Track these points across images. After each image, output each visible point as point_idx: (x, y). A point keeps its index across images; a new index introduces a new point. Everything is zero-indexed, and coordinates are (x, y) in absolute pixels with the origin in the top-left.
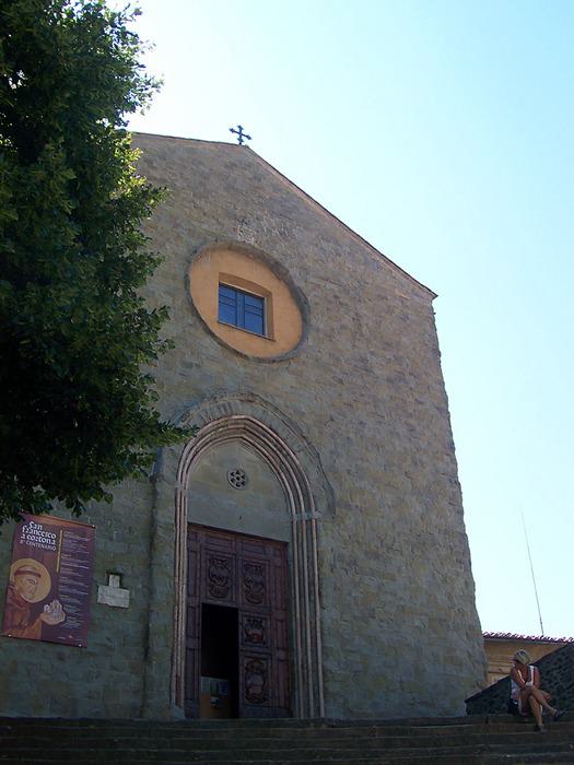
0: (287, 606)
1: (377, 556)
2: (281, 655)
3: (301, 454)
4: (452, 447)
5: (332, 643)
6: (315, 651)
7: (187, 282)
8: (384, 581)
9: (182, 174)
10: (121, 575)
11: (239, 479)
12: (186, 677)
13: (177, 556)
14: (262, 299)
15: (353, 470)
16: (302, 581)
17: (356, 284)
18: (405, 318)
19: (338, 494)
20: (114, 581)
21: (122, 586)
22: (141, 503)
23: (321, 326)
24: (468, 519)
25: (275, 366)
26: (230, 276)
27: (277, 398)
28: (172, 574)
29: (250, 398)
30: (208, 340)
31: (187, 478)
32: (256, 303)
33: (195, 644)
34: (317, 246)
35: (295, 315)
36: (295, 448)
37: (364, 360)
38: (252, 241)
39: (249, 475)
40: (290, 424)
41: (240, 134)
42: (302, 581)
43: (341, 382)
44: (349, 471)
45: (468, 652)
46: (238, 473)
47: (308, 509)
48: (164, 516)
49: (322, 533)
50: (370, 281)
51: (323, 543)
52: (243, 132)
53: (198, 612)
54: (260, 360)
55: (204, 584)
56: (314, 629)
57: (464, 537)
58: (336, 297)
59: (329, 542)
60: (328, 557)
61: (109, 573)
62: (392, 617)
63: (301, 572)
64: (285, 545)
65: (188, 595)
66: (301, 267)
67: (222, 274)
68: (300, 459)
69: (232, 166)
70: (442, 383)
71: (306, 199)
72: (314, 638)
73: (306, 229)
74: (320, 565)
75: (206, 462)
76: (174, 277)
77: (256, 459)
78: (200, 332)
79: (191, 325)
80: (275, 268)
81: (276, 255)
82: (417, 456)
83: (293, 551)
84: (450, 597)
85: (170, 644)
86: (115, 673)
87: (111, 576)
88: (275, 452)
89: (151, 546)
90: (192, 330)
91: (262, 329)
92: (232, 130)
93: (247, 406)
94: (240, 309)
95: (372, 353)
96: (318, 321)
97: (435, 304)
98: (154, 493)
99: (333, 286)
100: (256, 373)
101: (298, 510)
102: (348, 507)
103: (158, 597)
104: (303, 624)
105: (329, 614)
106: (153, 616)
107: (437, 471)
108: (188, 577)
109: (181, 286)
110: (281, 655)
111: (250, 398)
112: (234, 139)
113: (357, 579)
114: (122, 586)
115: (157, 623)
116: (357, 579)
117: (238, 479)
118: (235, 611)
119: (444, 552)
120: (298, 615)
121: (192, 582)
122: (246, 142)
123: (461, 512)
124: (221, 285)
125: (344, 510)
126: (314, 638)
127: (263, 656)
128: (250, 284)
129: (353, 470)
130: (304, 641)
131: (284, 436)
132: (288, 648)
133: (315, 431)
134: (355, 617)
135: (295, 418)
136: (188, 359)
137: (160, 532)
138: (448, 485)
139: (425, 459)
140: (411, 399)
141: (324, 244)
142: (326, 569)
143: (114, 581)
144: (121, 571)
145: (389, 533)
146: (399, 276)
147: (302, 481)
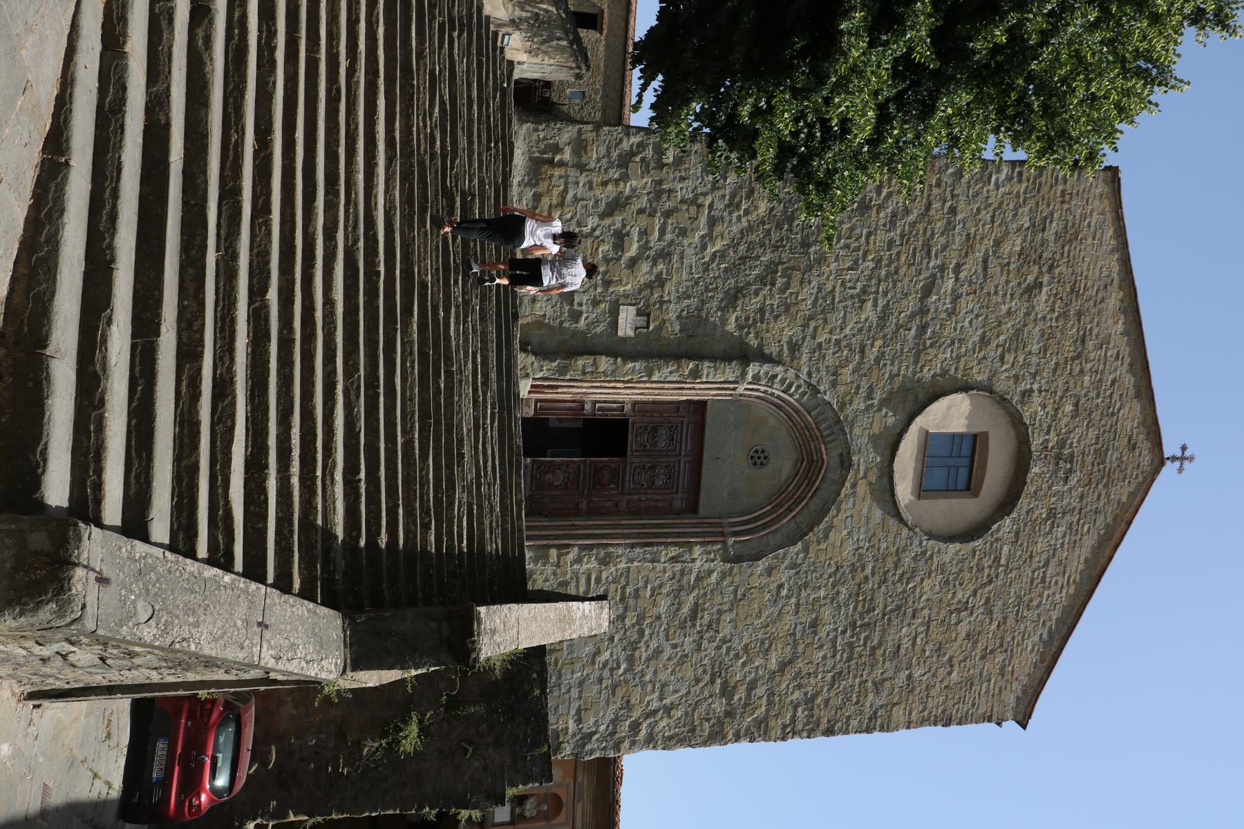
0: (635, 512)
2: (584, 505)
3: (793, 525)
14: (968, 488)
20: (641, 321)
25: (888, 497)
28: (655, 378)
32: (962, 483)
36: (799, 519)
38: (1035, 470)
41: (1183, 459)
45: (595, 733)
46: (765, 458)
47: (735, 534)
52: (1186, 463)
64: (693, 508)
65: (635, 403)
71: (1113, 543)
75: (772, 421)
77: (784, 475)
79: (917, 396)
90: (911, 398)
92: (1184, 448)
94: (951, 462)
108: (654, 402)
110: (584, 505)
112: (1170, 449)
118: (623, 453)
124: (975, 436)
128: (983, 468)
131: (812, 505)
132: (593, 512)
134: (623, 588)
142: (673, 551)
147: (765, 526)
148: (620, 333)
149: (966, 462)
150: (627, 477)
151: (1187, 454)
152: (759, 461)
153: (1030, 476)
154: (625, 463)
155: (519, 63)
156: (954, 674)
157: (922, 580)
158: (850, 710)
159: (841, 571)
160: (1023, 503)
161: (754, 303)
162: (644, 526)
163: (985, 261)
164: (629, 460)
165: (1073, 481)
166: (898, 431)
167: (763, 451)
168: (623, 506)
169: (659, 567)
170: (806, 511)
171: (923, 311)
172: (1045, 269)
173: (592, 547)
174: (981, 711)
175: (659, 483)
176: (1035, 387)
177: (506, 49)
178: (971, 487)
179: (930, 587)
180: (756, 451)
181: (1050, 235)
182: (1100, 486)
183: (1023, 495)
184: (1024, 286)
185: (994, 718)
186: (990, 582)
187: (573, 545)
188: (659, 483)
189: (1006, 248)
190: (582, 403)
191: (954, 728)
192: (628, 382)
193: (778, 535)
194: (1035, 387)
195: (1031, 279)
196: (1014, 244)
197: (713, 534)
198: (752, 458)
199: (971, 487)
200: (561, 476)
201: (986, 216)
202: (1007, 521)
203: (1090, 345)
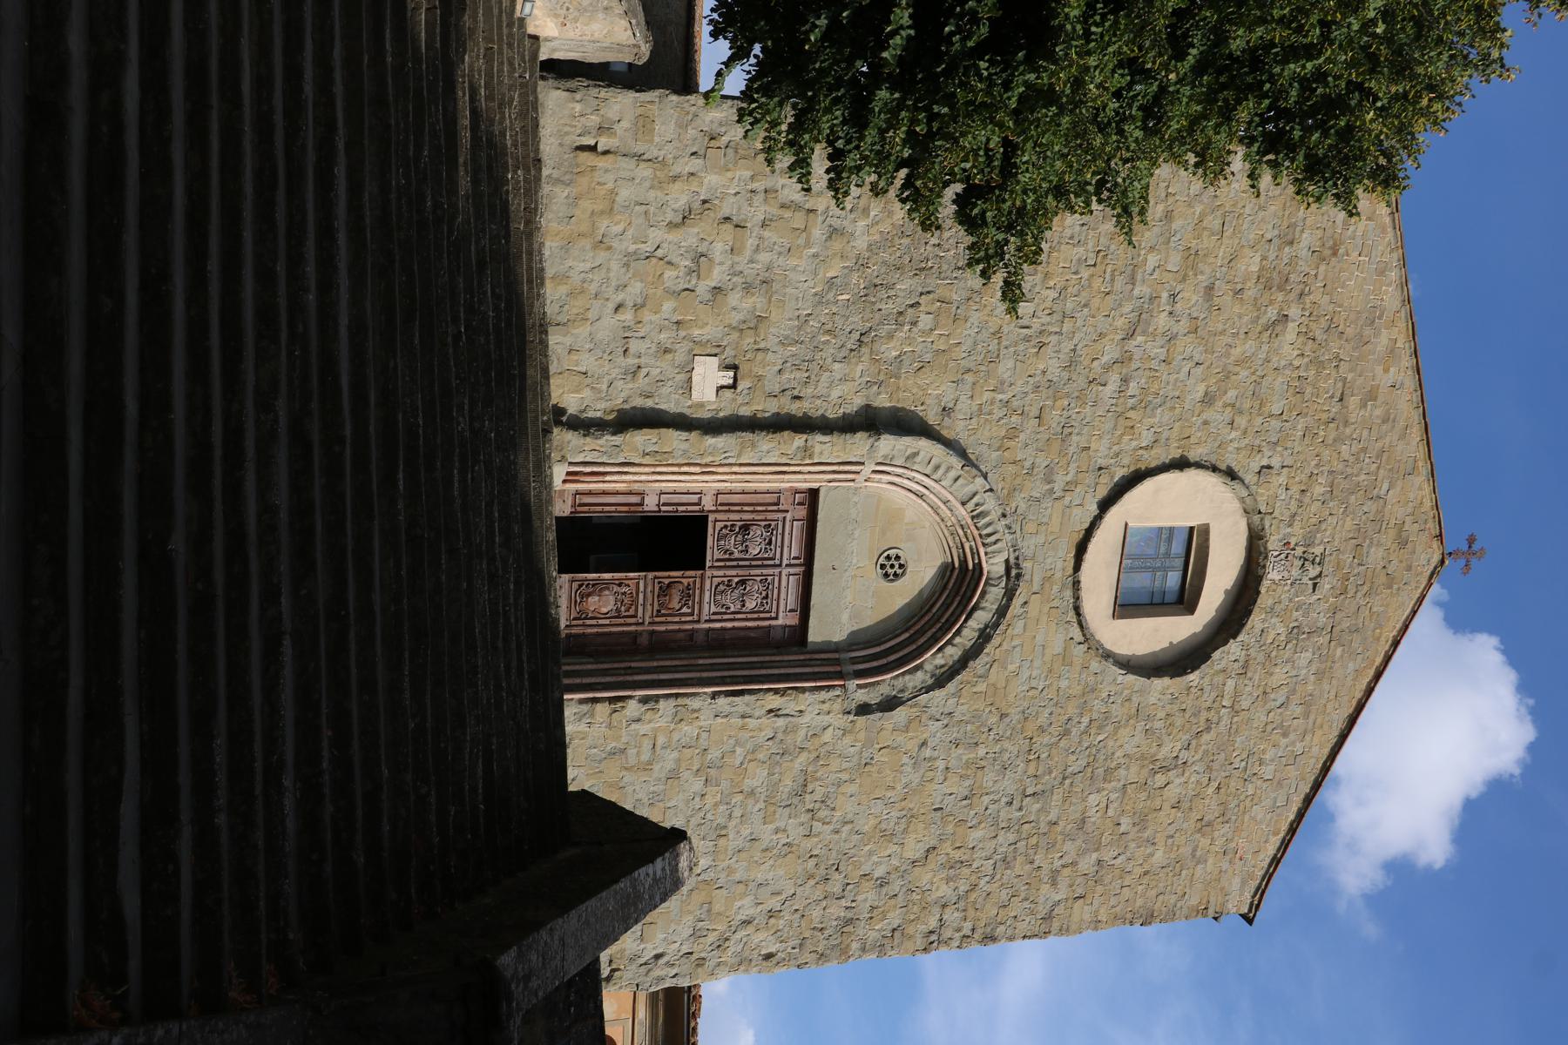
1: (802, 790)
7: (1181, 464)
8: (761, 805)
9: (1364, 450)
10: (734, 386)
15: (928, 753)
16: (751, 666)
20: (727, 378)
25: (1071, 616)
27: (1021, 624)
31: (880, 485)
33: (651, 504)
40: (985, 636)
42: (751, 666)
43: (1066, 733)
44: (924, 744)
46: (901, 566)
48: (826, 447)
49: (823, 695)
51: (808, 697)
62: (709, 816)
63: (762, 665)
66: (1246, 666)
67: (1205, 531)
73: (1320, 675)
74: (776, 691)
78: (1103, 492)
84: (747, 922)
86: (604, 387)
87: (731, 374)
88: (938, 620)
92: (1471, 541)
99: (1225, 721)
104: (687, 669)
107: (944, 906)
111: (1014, 572)
113: (761, 756)
115: (674, 440)
117: (892, 566)
119: (816, 913)
120: (701, 662)
124: (1192, 529)
125: (862, 735)
127: (640, 609)
129: (928, 753)
131: (965, 632)
133: (981, 687)
137: (799, 440)
138: (923, 928)
142: (774, 701)
143: (727, 378)
144: (739, 388)
149: (1179, 563)
150: (707, 598)
151: (1475, 547)
152: (890, 571)
153: (1265, 583)
154: (702, 577)
155: (547, 40)
156: (1159, 854)
157: (1116, 730)
158: (1017, 908)
159: (1007, 720)
160: (1256, 620)
161: (890, 350)
162: (730, 666)
163: (1210, 288)
164: (708, 573)
165: (1326, 585)
166: (1087, 525)
167: (898, 558)
169: (752, 723)
170: (957, 640)
171: (1124, 360)
172: (1293, 296)
173: (657, 698)
174: (1194, 901)
175: (750, 605)
177: (528, 21)
178: (1185, 601)
179: (1130, 740)
180: (888, 558)
181: (1302, 248)
182: (1359, 595)
183: (1256, 610)
184: (1263, 321)
185: (1211, 912)
186: (1208, 729)
187: (630, 697)
189: (1241, 266)
190: (642, 494)
192: (707, 465)
193: (919, 674)
195: (1272, 313)
196: (1251, 263)
198: (883, 566)
199: (1185, 601)
200: (612, 598)
201: (1213, 222)
203: (1353, 402)
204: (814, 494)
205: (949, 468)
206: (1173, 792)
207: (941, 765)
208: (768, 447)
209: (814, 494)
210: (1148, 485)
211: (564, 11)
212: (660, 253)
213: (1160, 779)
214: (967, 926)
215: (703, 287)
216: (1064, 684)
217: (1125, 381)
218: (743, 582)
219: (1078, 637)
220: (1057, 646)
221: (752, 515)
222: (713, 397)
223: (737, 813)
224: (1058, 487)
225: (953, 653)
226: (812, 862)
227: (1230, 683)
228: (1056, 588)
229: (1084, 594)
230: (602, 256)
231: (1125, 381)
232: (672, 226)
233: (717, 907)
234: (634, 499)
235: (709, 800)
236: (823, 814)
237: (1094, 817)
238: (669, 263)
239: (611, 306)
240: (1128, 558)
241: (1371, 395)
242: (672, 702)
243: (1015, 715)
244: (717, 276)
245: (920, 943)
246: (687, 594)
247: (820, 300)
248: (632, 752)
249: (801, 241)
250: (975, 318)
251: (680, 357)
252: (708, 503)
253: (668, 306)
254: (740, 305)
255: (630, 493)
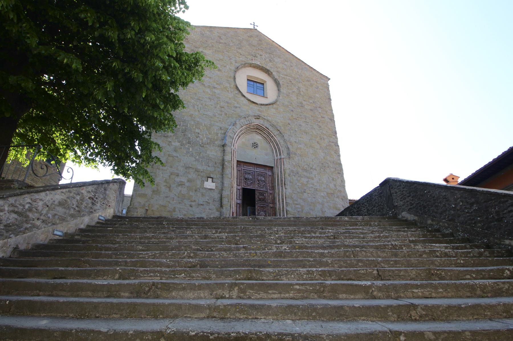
0: (273, 188)
1: (306, 170)
2: (271, 205)
4: (336, 133)
5: (289, 201)
6: (283, 204)
7: (235, 78)
11: (255, 145)
12: (236, 213)
13: (232, 173)
14: (263, 84)
16: (278, 180)
17: (298, 77)
18: (317, 88)
19: (291, 149)
20: (210, 180)
21: (212, 182)
22: (220, 154)
23: (285, 92)
24: (342, 158)
26: (251, 77)
28: (230, 177)
29: (258, 117)
30: (243, 98)
31: (236, 145)
32: (261, 86)
33: (239, 201)
34: (283, 63)
35: (275, 87)
36: (275, 134)
37: (301, 103)
38: (259, 63)
39: (259, 144)
40: (273, 126)
42: (278, 180)
43: (292, 111)
44: (295, 142)
47: (280, 155)
48: (228, 158)
49: (285, 163)
50: (304, 75)
51: (286, 166)
53: (241, 191)
54: (261, 105)
55: (243, 181)
56: (282, 196)
57: (340, 164)
58: (290, 81)
59: (288, 166)
60: (288, 171)
61: (208, 177)
64: (272, 167)
65: (237, 185)
68: (278, 138)
69: (251, 36)
70: (332, 110)
71: (279, 47)
72: (283, 199)
75: (243, 140)
76: (230, 77)
78: (240, 96)
80: (267, 72)
81: (268, 68)
82: (322, 136)
83: (275, 170)
85: (230, 201)
89: (223, 168)
90: (237, 95)
91: (250, 81)
93: (257, 120)
94: (255, 88)
95: (304, 100)
96: (283, 90)
97: (329, 82)
98: (224, 150)
100: (261, 109)
101: (277, 156)
102: (295, 154)
103: (225, 185)
105: (288, 191)
106: (224, 192)
109: (232, 80)
110: (271, 205)
112: (252, 27)
114: (212, 182)
115: (225, 193)
116: (299, 179)
118: (254, 190)
119: (333, 170)
121: (238, 181)
122: (256, 27)
123: (339, 156)
124: (248, 80)
125: (294, 155)
126: (283, 199)
128: (257, 78)
129: (297, 141)
130: (279, 200)
131: (271, 129)
132: (274, 203)
133: (283, 128)
135: (275, 124)
136: (236, 105)
137: (226, 163)
139: (325, 137)
140: (320, 116)
141: (286, 63)
142: (287, 175)
143: (210, 180)
145: (311, 163)
146: (315, 73)
147: (277, 145)
148: (214, 188)
149: (255, 84)
154: (257, 190)
168: (271, 192)
171: (209, 87)
175: (263, 179)
176: (234, 59)
188: (263, 179)
190: (237, 204)
191: (331, 98)
194: (234, 59)
197: (281, 162)
202: (274, 73)
203: (221, 41)
204: (238, 161)
205: (233, 129)
206: (304, 90)
207: (300, 139)
208: (228, 171)
209: (238, 161)
210: (238, 86)
211: (104, 205)
212: (177, 195)
213: (302, 93)
214: (333, 137)
215: (187, 184)
216: (282, 110)
217: (214, 88)
218: (258, 181)
219: (272, 106)
220: (273, 110)
221: (242, 177)
222: (215, 184)
223: (311, 186)
224: (238, 106)
225: (276, 133)
226: (322, 170)
227: (281, 76)
228: (261, 109)
229: (262, 103)
230: (177, 210)
231: (214, 88)
232: (170, 190)
233: (332, 192)
234: (238, 205)
235: (309, 192)
236: (311, 166)
237: (309, 107)
238: (180, 192)
239: (190, 208)
240: (254, 93)
241: (220, 37)
242: (287, 199)
243: (290, 122)
244: (184, 179)
245: (337, 148)
246: (262, 194)
247: (192, 155)
248: (298, 210)
249: (176, 158)
250: (198, 120)
251: (204, 191)
252: (239, 187)
253: (191, 193)
254: (192, 175)
255: (237, 207)
